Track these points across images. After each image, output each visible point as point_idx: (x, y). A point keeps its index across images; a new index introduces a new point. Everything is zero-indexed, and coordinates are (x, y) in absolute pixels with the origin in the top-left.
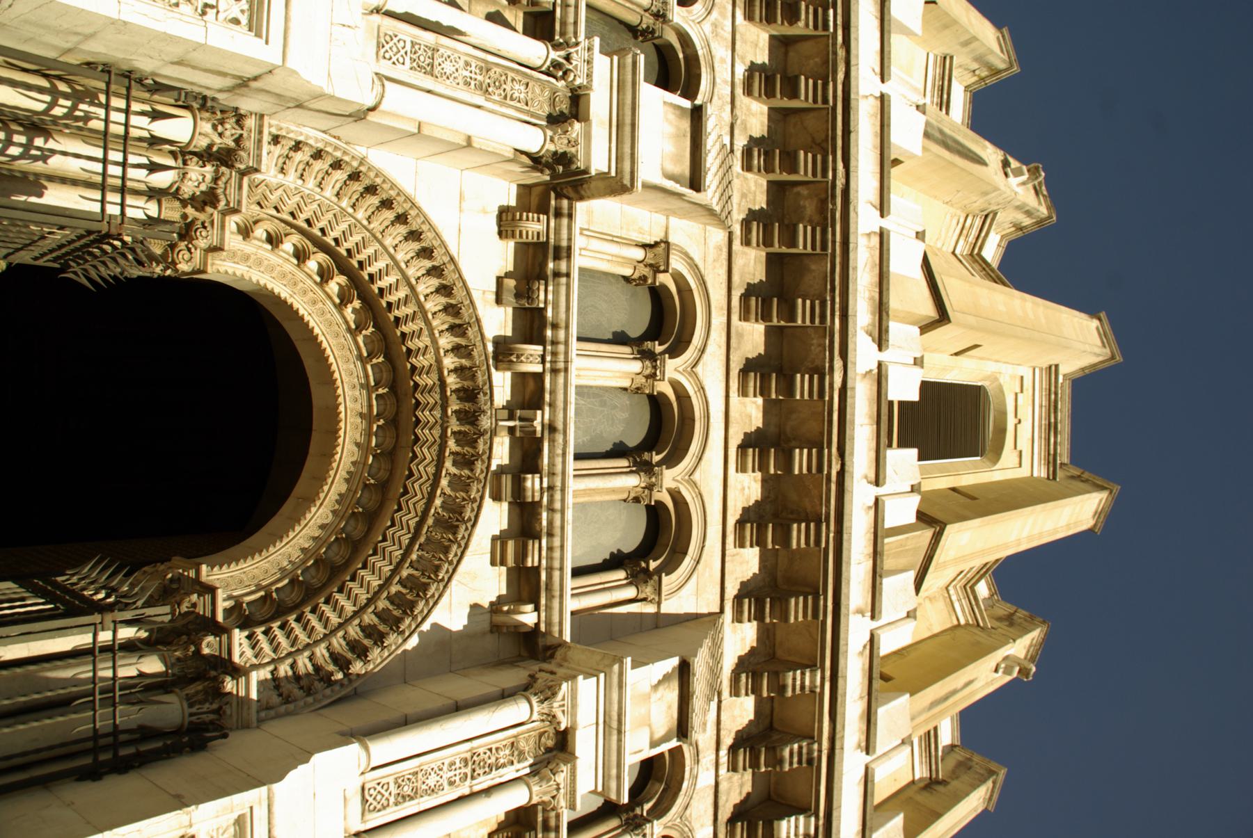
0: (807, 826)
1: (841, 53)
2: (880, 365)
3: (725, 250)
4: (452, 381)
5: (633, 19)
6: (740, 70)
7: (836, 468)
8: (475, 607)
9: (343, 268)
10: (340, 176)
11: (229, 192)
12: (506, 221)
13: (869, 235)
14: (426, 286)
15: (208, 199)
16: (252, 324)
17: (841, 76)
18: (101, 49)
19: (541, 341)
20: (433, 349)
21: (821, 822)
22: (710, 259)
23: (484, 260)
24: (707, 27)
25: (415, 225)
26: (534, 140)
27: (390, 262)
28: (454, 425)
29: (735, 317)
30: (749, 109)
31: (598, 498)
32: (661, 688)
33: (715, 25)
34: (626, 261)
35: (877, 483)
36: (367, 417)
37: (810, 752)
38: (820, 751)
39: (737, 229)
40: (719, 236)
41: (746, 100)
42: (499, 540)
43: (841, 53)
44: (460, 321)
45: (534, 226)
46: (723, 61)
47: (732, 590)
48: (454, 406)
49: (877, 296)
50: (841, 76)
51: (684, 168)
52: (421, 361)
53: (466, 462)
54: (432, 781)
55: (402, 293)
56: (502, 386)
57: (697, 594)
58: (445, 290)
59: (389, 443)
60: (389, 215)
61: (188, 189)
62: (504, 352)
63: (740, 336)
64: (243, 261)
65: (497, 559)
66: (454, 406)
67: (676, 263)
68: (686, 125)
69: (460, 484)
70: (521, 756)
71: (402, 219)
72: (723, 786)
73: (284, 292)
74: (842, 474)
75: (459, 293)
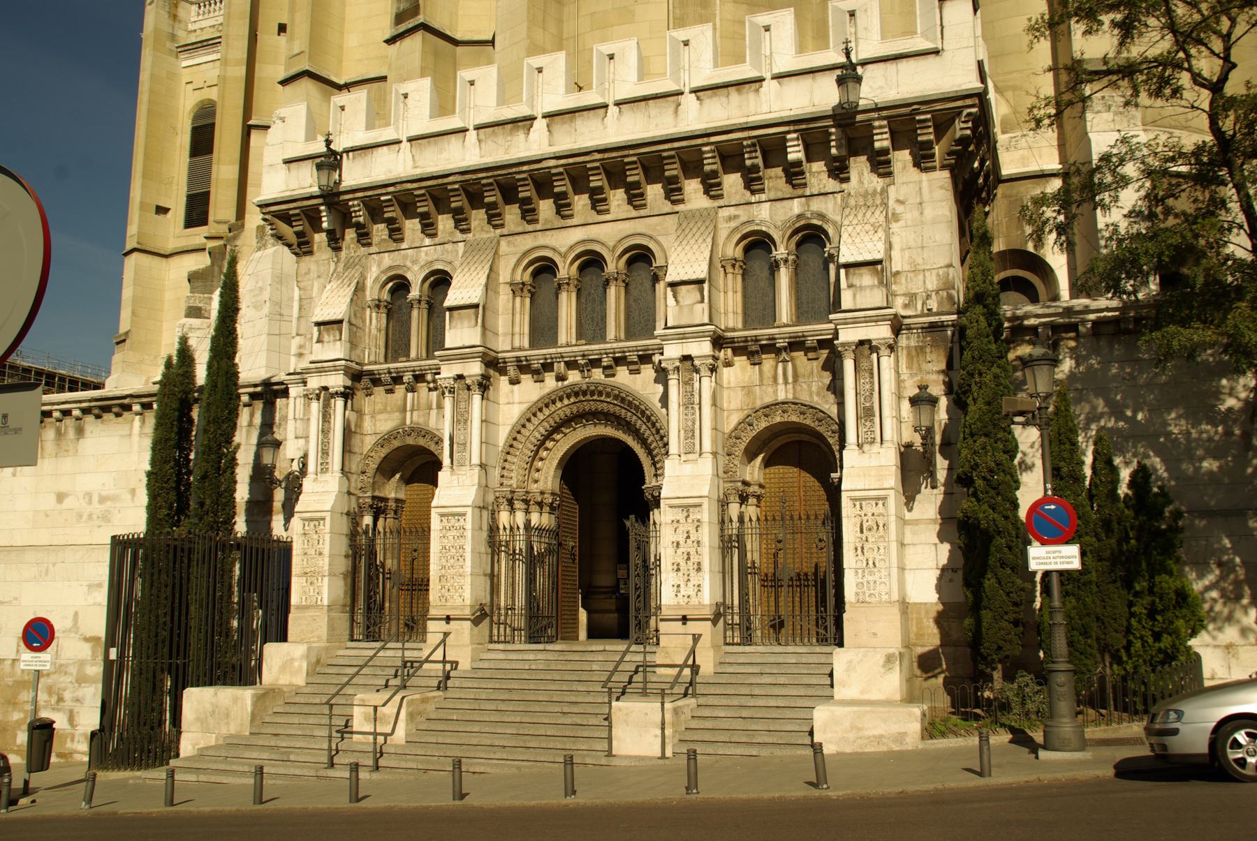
0: (792, 140)
1: (399, 188)
2: (544, 117)
3: (510, 238)
4: (572, 400)
5: (425, 312)
6: (427, 241)
7: (598, 156)
8: (656, 381)
9: (543, 443)
10: (509, 457)
11: (520, 493)
12: (514, 382)
13: (480, 141)
14: (541, 416)
15: (526, 502)
16: (572, 467)
17: (409, 186)
18: (484, 548)
19: (552, 364)
20: (563, 408)
21: (792, 128)
22: (512, 249)
23: (529, 391)
24: (416, 268)
25: (519, 427)
26: (477, 398)
27: (535, 431)
28: (588, 397)
29: (539, 227)
30: (444, 231)
31: (622, 307)
32: (680, 299)
33: (414, 262)
34: (522, 303)
35: (606, 106)
36: (595, 424)
37: (748, 146)
38: (750, 138)
39: (498, 231)
40: (503, 242)
41: (439, 233)
42: (631, 372)
43: (399, 188)
44: (549, 401)
45: (512, 371)
46: (426, 254)
47: (668, 207)
48: (581, 398)
49: (509, 126)
50: (409, 186)
51: (472, 311)
52: (568, 412)
53: (600, 394)
54: (690, 423)
55: (545, 424)
56: (574, 377)
57: (667, 234)
58: (541, 410)
59: (602, 417)
60: (518, 436)
61: (524, 506)
62: (560, 378)
63: (546, 221)
64: (547, 478)
65: (638, 372)
66: (581, 398)
67: (518, 279)
68: (456, 313)
69: (608, 395)
70: (692, 379)
71: (519, 432)
72: (772, 195)
73: (556, 462)
74: (599, 151)
75: (540, 405)
